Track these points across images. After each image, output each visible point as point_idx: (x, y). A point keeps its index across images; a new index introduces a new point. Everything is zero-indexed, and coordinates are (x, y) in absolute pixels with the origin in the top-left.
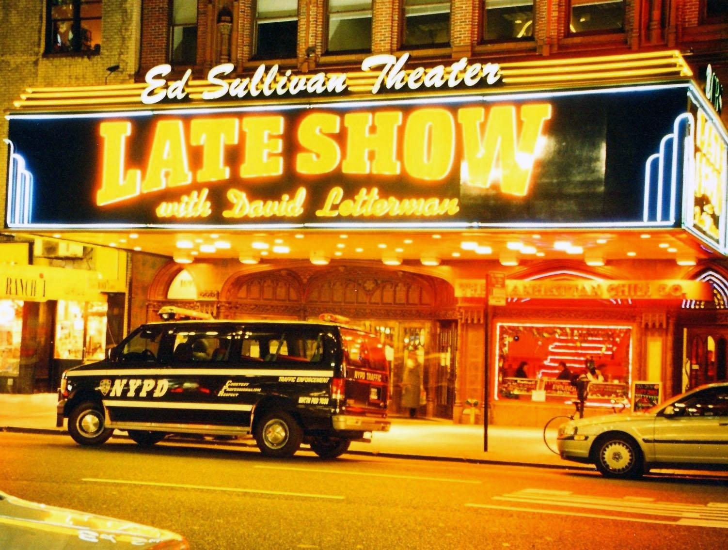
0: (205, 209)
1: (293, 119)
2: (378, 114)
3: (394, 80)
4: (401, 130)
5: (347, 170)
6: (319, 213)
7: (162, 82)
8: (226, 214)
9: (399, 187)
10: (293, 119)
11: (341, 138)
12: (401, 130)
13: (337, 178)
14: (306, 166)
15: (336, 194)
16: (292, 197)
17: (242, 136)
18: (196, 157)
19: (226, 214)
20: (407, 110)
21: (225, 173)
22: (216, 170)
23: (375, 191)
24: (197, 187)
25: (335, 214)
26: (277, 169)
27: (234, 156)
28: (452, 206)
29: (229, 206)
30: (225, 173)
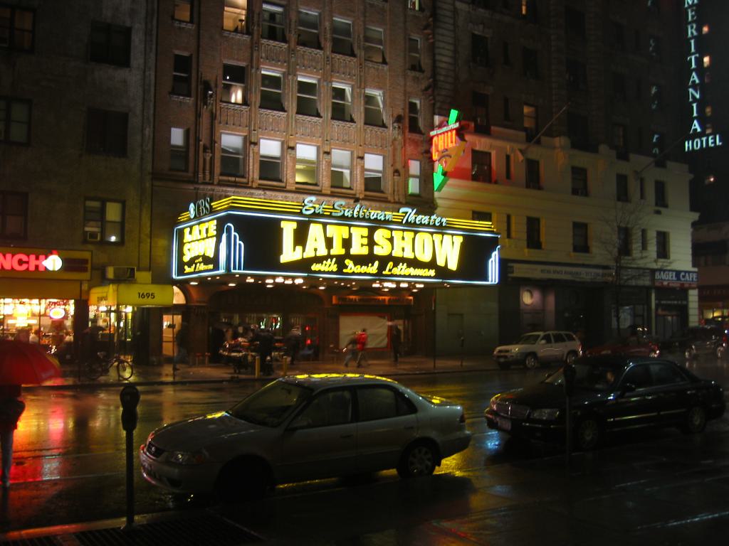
0: (334, 268)
1: (372, 231)
2: (405, 232)
3: (412, 219)
4: (414, 239)
5: (394, 254)
6: (384, 273)
7: (311, 205)
8: (345, 271)
9: (414, 263)
10: (372, 231)
11: (391, 240)
12: (414, 239)
13: (390, 258)
14: (378, 251)
15: (390, 264)
16: (373, 265)
17: (350, 235)
18: (329, 242)
19: (345, 271)
20: (416, 232)
21: (342, 252)
22: (338, 250)
23: (405, 264)
24: (329, 257)
25: (390, 273)
26: (365, 251)
27: (347, 243)
28: (432, 273)
29: (346, 267)
30: (342, 252)
